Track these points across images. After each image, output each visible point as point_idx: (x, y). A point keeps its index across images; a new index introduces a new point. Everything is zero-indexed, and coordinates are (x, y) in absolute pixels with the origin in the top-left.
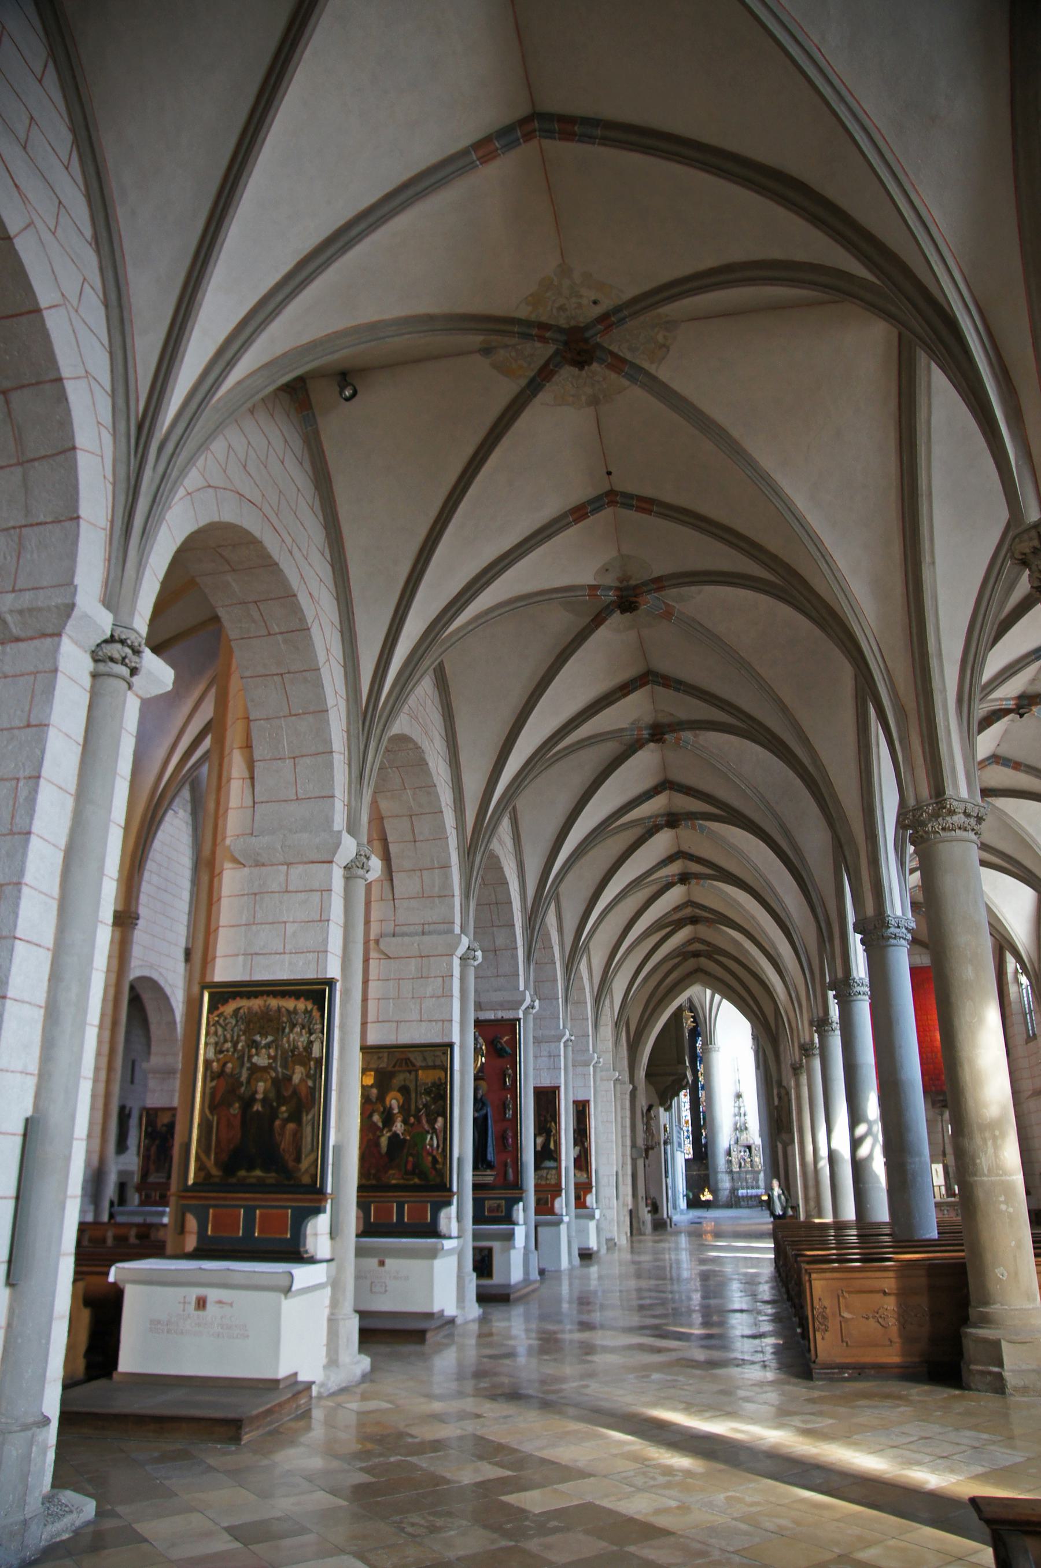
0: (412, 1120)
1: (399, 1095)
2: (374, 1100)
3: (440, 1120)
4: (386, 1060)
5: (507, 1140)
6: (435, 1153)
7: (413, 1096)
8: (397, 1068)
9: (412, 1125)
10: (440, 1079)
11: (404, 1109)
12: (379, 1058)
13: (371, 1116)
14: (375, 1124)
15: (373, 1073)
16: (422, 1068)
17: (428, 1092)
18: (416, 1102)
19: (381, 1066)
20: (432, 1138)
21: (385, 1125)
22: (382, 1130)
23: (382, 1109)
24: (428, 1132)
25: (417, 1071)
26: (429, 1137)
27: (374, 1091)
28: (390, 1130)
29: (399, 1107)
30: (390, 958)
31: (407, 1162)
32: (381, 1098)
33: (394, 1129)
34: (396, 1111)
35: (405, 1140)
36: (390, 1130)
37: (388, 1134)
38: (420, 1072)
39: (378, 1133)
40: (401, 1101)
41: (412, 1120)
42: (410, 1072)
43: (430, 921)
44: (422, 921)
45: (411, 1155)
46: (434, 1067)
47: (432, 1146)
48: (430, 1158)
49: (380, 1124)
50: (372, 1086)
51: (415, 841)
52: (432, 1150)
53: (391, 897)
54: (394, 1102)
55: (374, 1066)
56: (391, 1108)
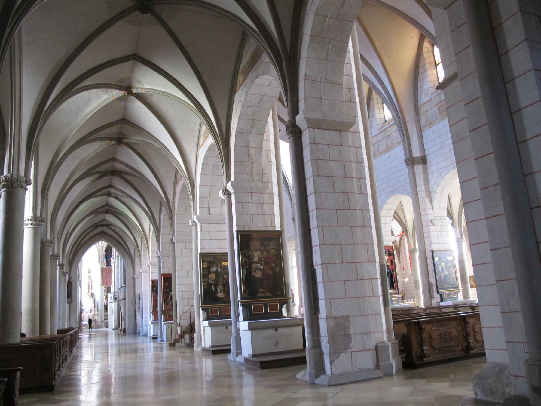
1: (444, 264)
14: (440, 271)
16: (448, 256)
17: (450, 263)
28: (444, 273)
30: (434, 225)
34: (444, 268)
41: (448, 270)
48: (453, 280)
49: (441, 272)
53: (432, 208)
56: (443, 267)
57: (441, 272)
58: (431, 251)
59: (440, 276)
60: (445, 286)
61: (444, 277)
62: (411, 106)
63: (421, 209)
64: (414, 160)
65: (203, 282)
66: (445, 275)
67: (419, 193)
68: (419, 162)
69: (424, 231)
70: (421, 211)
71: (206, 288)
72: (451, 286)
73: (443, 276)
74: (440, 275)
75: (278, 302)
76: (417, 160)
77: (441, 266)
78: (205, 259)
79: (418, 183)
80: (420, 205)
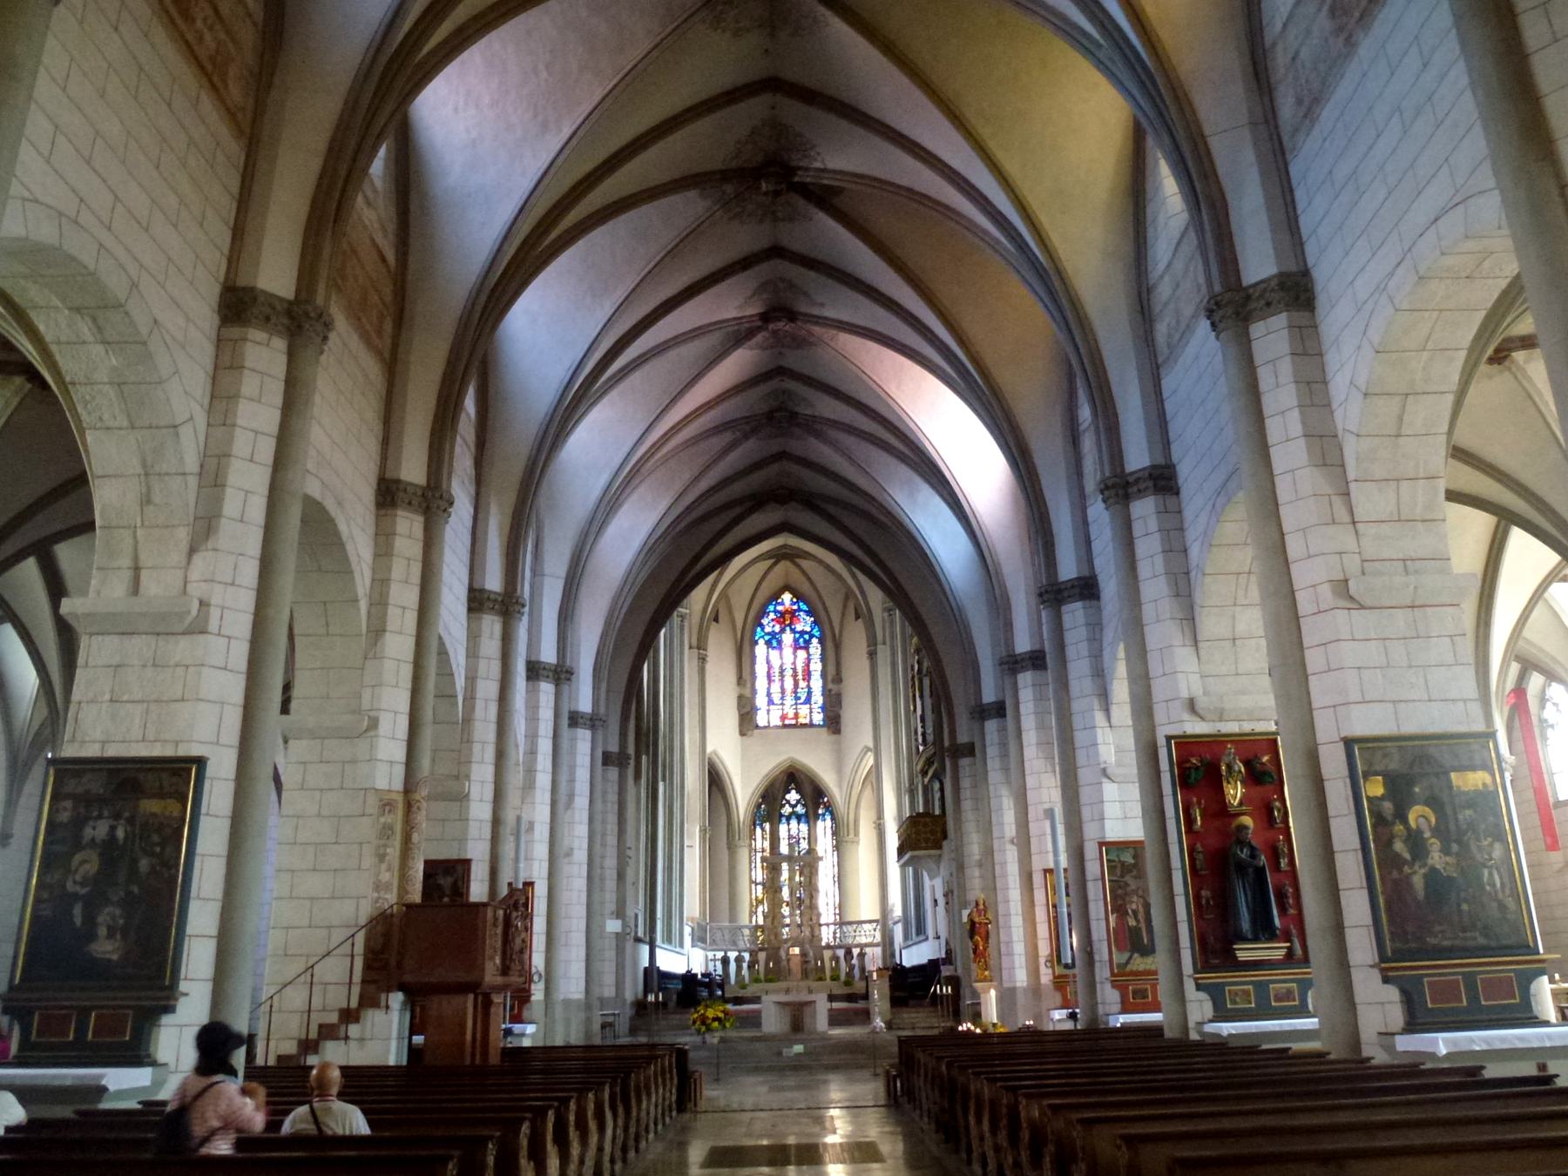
0: (1455, 847)
1: (1427, 809)
2: (1390, 818)
3: (1497, 846)
4: (1396, 757)
5: (1287, 897)
6: (1500, 895)
7: (1449, 810)
8: (1416, 770)
9: (1457, 855)
10: (1484, 785)
11: (1440, 831)
12: (1385, 756)
13: (1390, 843)
14: (1397, 856)
15: (1380, 778)
16: (1455, 770)
18: (1456, 819)
19: (1393, 766)
20: (1491, 874)
21: (1414, 859)
22: (1411, 864)
23: (1405, 833)
24: (1485, 866)
25: (1446, 773)
26: (1486, 872)
27: (1388, 806)
28: (1425, 865)
29: (1431, 829)
30: (1363, 607)
31: (1460, 911)
32: (1401, 816)
33: (1430, 862)
34: (1427, 834)
35: (1450, 878)
36: (1425, 865)
37: (1423, 871)
38: (1453, 775)
39: (1406, 869)
40: (1433, 820)
41: (1455, 847)
42: (1437, 775)
43: (1413, 555)
44: (1401, 556)
45: (1466, 900)
46: (1473, 768)
47: (1494, 885)
48: (1495, 905)
49: (1407, 856)
50: (1382, 798)
51: (1398, 436)
52: (1496, 892)
53: (1347, 519)
54: (1421, 820)
55: (1378, 768)
56: (1419, 832)
57: (1407, 856)
58: (1341, 745)
59: (1396, 882)
60: (1431, 941)
61: (1427, 885)
62: (1231, 60)
63: (1285, 529)
64: (1248, 298)
65: (40, 885)
66: (1433, 876)
67: (1274, 452)
68: (1268, 304)
69: (1307, 641)
70: (1289, 539)
71: (47, 913)
72: (1482, 941)
73: (1418, 881)
74: (1395, 874)
75: (129, 1007)
76: (1261, 296)
77: (1405, 821)
78: (71, 786)
79: (1269, 404)
80: (1283, 511)
